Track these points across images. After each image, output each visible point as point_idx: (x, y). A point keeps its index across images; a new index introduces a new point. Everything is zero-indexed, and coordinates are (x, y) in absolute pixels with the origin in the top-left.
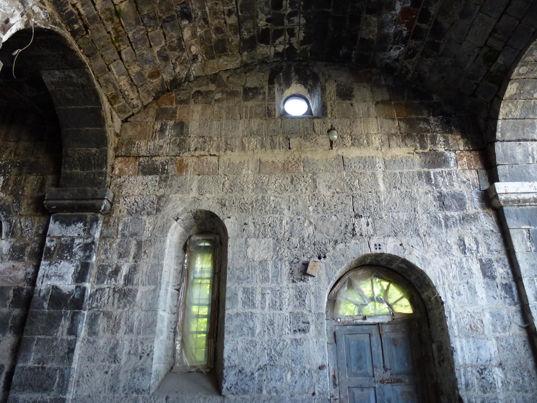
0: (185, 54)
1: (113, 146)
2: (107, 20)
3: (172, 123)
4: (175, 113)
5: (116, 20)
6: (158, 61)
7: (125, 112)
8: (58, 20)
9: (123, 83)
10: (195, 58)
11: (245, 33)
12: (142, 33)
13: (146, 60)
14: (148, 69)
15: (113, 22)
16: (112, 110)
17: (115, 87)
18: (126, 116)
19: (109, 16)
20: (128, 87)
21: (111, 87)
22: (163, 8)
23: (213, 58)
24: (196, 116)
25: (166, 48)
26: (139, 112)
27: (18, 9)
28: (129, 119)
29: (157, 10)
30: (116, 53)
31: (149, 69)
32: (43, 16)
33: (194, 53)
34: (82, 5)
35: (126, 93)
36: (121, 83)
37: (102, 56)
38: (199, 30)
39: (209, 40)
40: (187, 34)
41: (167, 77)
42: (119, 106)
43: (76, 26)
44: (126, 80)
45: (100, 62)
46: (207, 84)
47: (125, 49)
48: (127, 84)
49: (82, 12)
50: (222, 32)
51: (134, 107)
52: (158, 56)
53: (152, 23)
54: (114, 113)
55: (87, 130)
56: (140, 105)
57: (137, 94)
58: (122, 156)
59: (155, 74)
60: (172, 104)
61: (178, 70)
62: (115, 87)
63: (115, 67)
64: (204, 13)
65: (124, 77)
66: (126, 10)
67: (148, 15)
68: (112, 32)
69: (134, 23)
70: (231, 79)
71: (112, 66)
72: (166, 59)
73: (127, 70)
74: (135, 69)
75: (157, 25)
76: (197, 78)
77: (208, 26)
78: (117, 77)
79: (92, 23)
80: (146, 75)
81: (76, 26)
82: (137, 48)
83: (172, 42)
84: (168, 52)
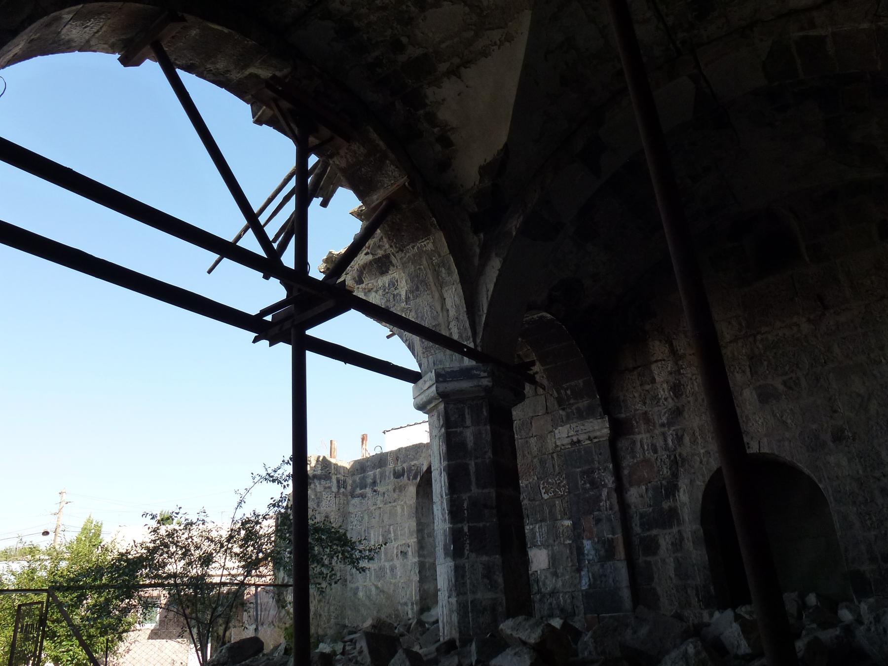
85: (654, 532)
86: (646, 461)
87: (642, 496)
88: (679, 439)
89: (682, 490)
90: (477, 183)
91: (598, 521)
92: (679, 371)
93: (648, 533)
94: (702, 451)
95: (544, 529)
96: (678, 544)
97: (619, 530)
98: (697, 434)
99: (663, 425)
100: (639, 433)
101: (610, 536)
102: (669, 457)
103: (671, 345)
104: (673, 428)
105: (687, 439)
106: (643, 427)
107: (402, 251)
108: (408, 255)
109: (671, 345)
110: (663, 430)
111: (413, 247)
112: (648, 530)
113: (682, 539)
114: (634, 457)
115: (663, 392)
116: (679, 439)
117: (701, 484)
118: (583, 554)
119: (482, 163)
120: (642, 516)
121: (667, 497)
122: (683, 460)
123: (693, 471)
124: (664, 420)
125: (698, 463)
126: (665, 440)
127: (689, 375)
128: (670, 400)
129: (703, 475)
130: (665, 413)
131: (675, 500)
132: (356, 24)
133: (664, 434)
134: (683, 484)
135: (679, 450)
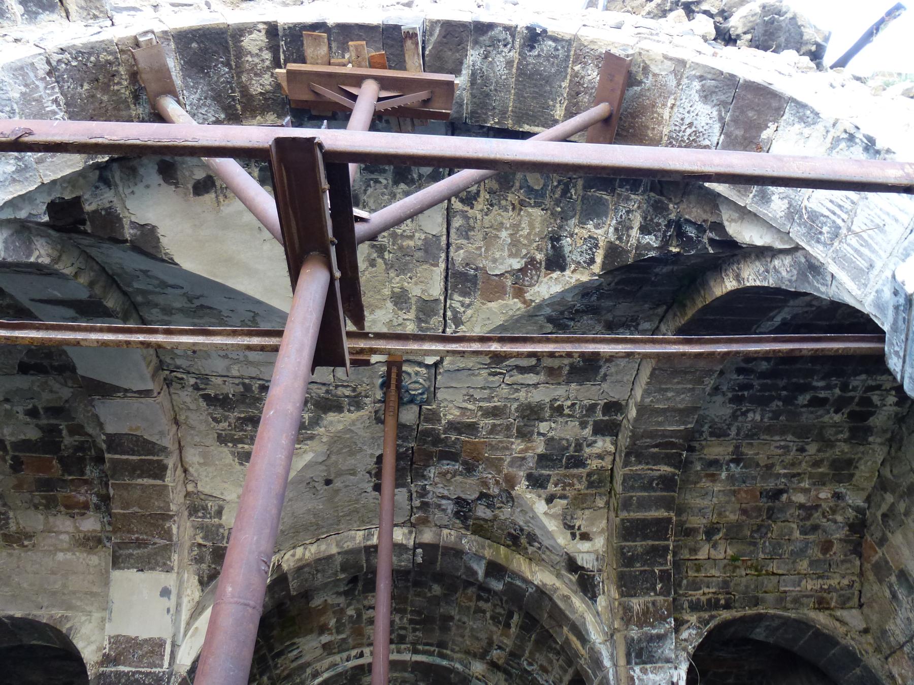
0: (824, 505)
1: (871, 650)
2: (734, 572)
3: (893, 579)
4: (887, 562)
5: (739, 563)
6: (811, 537)
7: (849, 599)
8: (706, 615)
9: (810, 585)
10: (837, 496)
11: (840, 436)
12: (767, 544)
13: (801, 550)
14: (815, 552)
15: (739, 567)
16: (833, 613)
17: (807, 596)
18: (856, 600)
19: (731, 568)
20: (820, 581)
21: (805, 600)
22: (754, 515)
23: (852, 475)
24: (906, 552)
25: (801, 524)
26: (862, 585)
27: (670, 668)
28: (862, 601)
29: (753, 521)
30: (772, 577)
31: (815, 550)
32: (694, 632)
33: (829, 496)
34: (708, 587)
35: (826, 587)
36: (809, 587)
37: (766, 592)
38: (802, 485)
39: (823, 475)
40: (800, 498)
41: (839, 534)
42: (836, 602)
43: (722, 602)
44: (809, 581)
45: (770, 597)
46: (884, 499)
47: (773, 567)
48: (815, 582)
49: (714, 590)
50: (822, 461)
51: (851, 586)
52: (806, 534)
53: (764, 530)
54: (838, 613)
55: (834, 654)
56: (855, 578)
57: (837, 575)
58: (890, 655)
59: (827, 546)
60: (877, 552)
61: (839, 518)
62: (807, 596)
63: (786, 586)
64: (785, 475)
65: (804, 582)
66: (735, 550)
67: (752, 532)
68: (748, 572)
69: (752, 548)
70: (895, 472)
71: (782, 589)
72: (815, 528)
73: (799, 574)
74: (803, 566)
75: (770, 525)
76: (868, 499)
77: (805, 474)
78: (798, 589)
79: (728, 587)
80: (821, 556)
81: (722, 602)
82: (781, 555)
83: (799, 516)
84: (808, 523)
90: (133, 219)
107: (49, 73)
108: (41, 85)
111: (56, 101)
119: (161, 231)
132: (403, 186)
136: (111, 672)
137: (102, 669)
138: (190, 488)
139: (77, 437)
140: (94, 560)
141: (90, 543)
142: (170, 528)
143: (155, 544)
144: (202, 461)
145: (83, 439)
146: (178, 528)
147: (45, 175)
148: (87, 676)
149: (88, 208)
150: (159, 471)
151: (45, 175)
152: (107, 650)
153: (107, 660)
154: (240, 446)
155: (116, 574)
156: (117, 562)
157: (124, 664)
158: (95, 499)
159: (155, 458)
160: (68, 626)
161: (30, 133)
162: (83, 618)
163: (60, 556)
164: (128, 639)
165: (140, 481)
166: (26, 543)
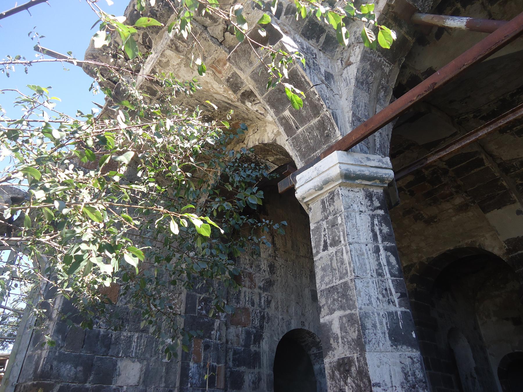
85: (242, 369)
86: (246, 310)
87: (237, 336)
88: (268, 302)
89: (264, 340)
90: (422, 72)
91: (207, 347)
92: (275, 257)
93: (238, 369)
94: (280, 317)
95: (144, 341)
96: (256, 383)
97: (223, 361)
98: (279, 304)
99: (260, 288)
100: (244, 286)
101: (215, 364)
102: (260, 312)
103: (273, 238)
104: (266, 293)
105: (273, 304)
106: (248, 283)
109: (273, 238)
110: (260, 291)
111: (379, 56)
112: (238, 366)
113: (260, 379)
114: (238, 303)
115: (264, 266)
116: (268, 302)
117: (277, 339)
118: (187, 376)
120: (235, 353)
121: (255, 343)
122: (269, 319)
123: (273, 328)
124: (261, 284)
125: (277, 324)
126: (260, 299)
127: (280, 263)
128: (267, 273)
129: (278, 334)
130: (263, 280)
131: (259, 347)
133: (260, 294)
134: (266, 335)
135: (266, 310)
136: (516, 255)
137: (510, 256)
138: (499, 161)
139: (430, 170)
140: (470, 214)
141: (463, 208)
142: (502, 184)
143: (498, 194)
144: (497, 147)
145: (432, 169)
146: (506, 182)
147: (392, 85)
148: (504, 261)
149: (404, 83)
150: (481, 162)
151: (392, 85)
152: (507, 247)
153: (509, 251)
154: (515, 128)
155: (488, 215)
156: (485, 210)
157: (520, 250)
158: (454, 190)
159: (474, 158)
160: (478, 244)
161: (435, 84)
162: (482, 239)
163: (454, 219)
164: (515, 239)
165: (473, 172)
166: (435, 220)
